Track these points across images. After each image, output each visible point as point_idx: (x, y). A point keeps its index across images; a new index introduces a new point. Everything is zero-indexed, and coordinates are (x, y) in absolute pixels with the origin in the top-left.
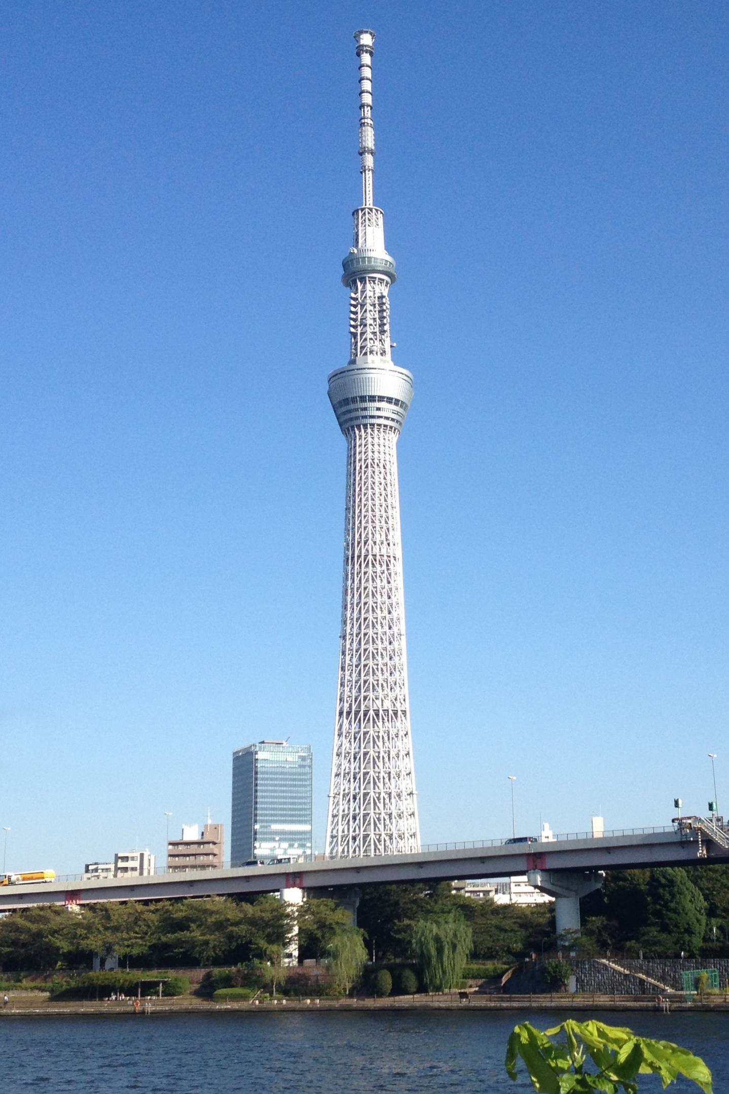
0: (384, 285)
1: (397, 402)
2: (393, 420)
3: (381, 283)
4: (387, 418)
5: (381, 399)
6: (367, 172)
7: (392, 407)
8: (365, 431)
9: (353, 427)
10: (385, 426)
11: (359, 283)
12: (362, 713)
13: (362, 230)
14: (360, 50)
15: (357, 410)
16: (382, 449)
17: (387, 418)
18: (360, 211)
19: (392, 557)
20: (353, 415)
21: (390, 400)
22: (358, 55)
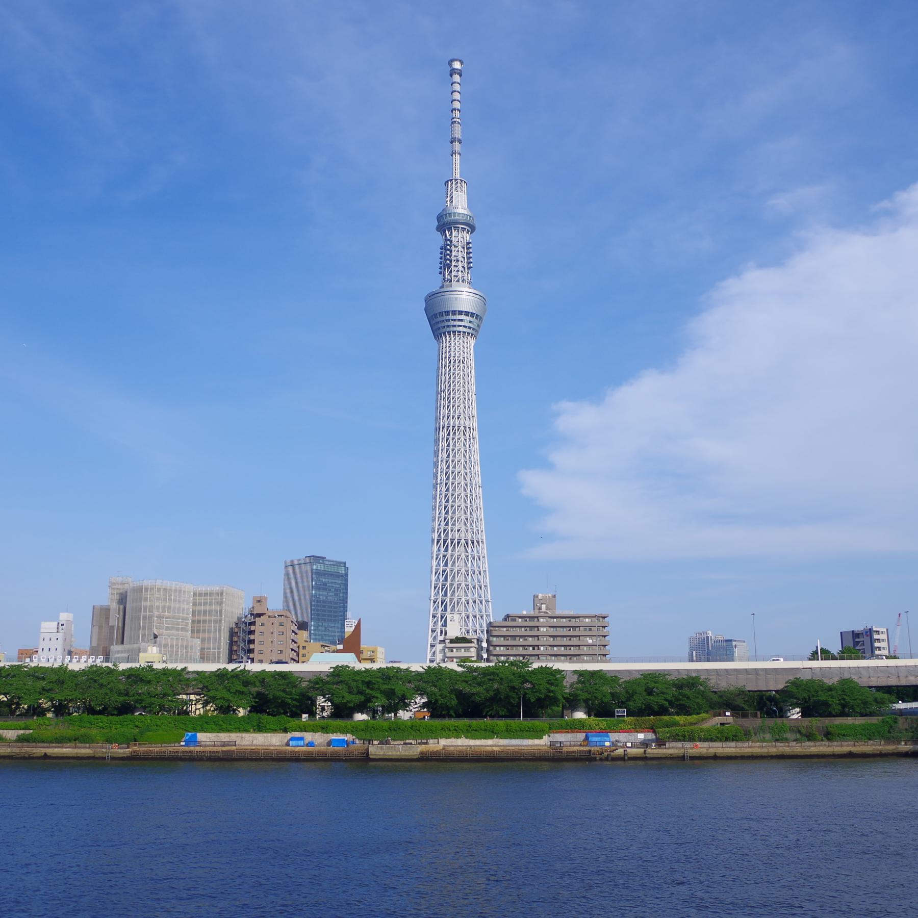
0: (465, 232)
1: (472, 315)
2: (470, 328)
3: (463, 231)
4: (465, 327)
5: (461, 313)
6: (457, 154)
7: (469, 318)
8: (449, 337)
9: (445, 333)
10: (464, 332)
11: (447, 232)
12: (449, 541)
13: (455, 194)
14: (453, 72)
15: (448, 320)
16: (465, 350)
17: (465, 327)
18: (449, 182)
19: (467, 428)
20: (443, 324)
21: (467, 313)
22: (451, 75)
